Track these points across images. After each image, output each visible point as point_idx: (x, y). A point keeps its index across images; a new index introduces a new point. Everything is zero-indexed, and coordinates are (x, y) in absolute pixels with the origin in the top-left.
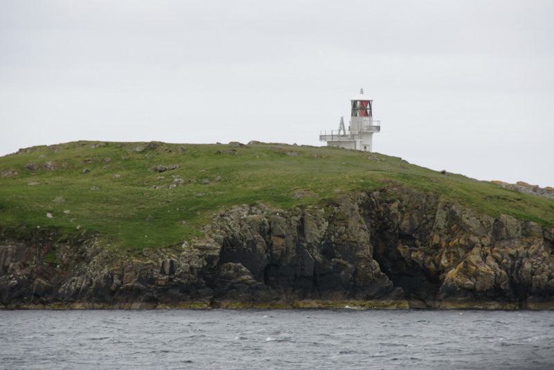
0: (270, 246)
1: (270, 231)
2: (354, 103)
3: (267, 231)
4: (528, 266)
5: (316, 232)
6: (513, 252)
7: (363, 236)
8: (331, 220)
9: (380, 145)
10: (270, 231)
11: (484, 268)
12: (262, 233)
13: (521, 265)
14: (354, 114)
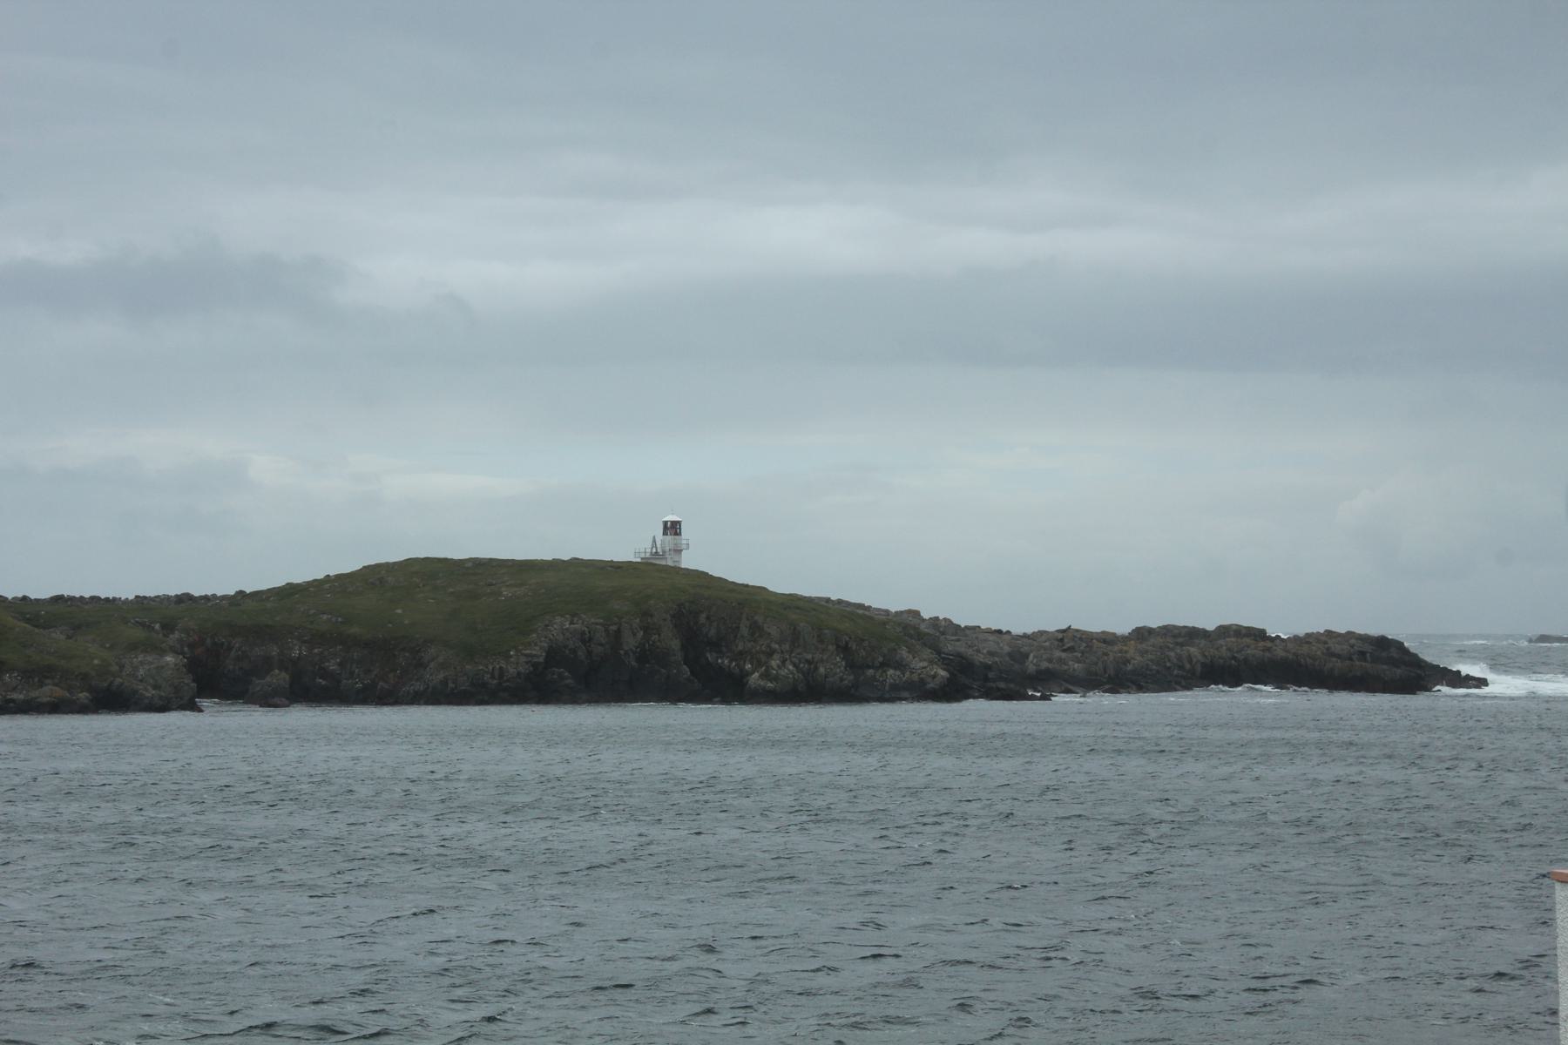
0: (590, 653)
1: (590, 639)
2: (665, 523)
3: (586, 639)
4: (822, 670)
5: (630, 642)
6: (809, 657)
7: (675, 644)
8: (646, 629)
9: (689, 561)
10: (590, 639)
11: (784, 672)
12: (583, 641)
13: (816, 668)
14: (665, 533)
